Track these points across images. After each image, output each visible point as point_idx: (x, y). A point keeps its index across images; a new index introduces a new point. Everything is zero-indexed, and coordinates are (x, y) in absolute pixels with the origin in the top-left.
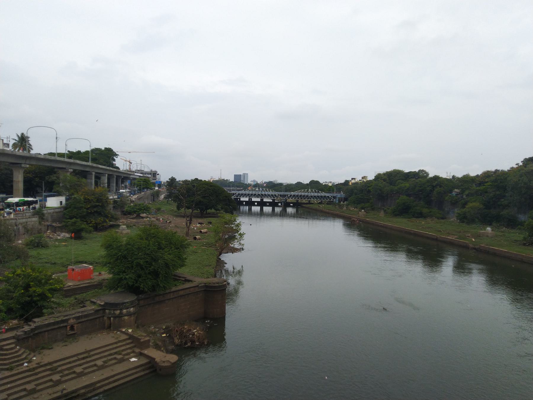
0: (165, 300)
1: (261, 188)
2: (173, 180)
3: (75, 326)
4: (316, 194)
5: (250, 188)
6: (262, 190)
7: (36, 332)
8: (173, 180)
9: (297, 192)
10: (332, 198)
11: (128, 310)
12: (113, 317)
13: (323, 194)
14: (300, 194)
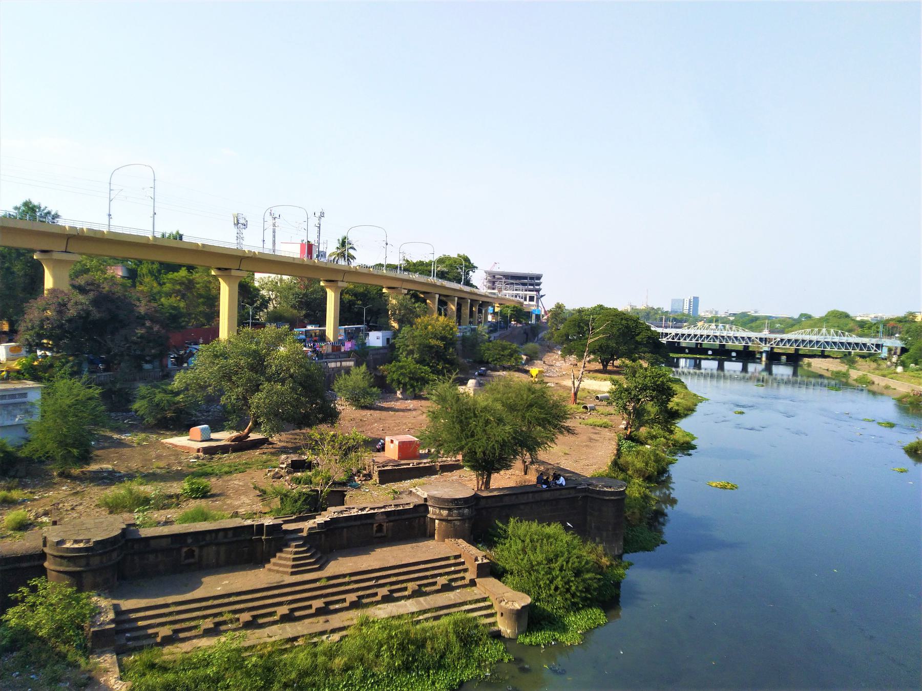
0: (519, 504)
1: (720, 325)
2: (559, 307)
3: (385, 525)
4: (837, 339)
5: (700, 324)
6: (722, 327)
7: (331, 527)
8: (559, 307)
9: (796, 332)
10: (873, 348)
11: (461, 511)
12: (439, 520)
13: (854, 339)
14: (800, 337)
